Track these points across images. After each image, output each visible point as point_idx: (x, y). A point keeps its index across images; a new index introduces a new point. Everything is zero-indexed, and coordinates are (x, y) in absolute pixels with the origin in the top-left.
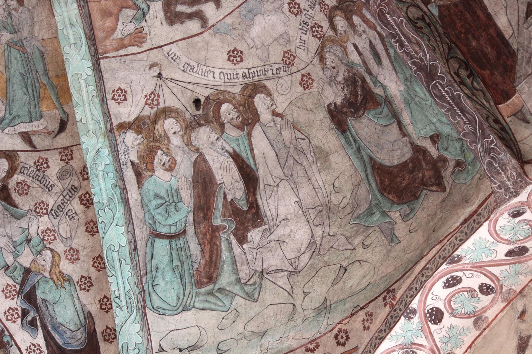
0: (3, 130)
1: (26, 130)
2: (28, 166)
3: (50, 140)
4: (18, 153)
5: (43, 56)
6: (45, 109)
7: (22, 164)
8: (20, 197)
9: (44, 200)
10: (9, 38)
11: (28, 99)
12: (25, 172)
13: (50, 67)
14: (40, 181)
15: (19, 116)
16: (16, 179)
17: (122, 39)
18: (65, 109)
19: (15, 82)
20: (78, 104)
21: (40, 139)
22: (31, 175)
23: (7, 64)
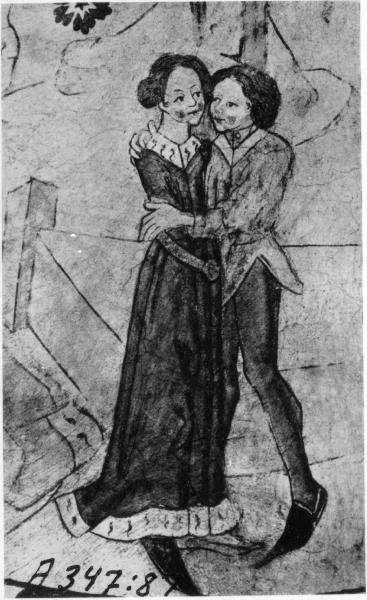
1: (167, 532)
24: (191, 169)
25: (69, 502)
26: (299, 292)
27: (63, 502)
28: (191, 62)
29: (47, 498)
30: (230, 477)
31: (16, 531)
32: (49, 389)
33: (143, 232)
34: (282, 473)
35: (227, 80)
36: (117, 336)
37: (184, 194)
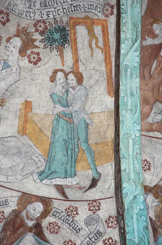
0: (41, 181)
1: (61, 184)
2: (60, 212)
3: (81, 194)
4: (53, 200)
5: (88, 127)
6: (79, 169)
7: (55, 209)
8: (51, 235)
9: (72, 240)
11: (67, 159)
12: (57, 216)
13: (91, 136)
14: (69, 224)
15: (56, 172)
16: (49, 220)
17: (152, 124)
20: (124, 157)
22: (62, 218)
23: (54, 131)
25: (36, 175)
26: (92, 125)
27: (34, 175)
28: (62, 70)
29: (30, 174)
30: (78, 171)
34: (90, 169)
37: (63, 103)
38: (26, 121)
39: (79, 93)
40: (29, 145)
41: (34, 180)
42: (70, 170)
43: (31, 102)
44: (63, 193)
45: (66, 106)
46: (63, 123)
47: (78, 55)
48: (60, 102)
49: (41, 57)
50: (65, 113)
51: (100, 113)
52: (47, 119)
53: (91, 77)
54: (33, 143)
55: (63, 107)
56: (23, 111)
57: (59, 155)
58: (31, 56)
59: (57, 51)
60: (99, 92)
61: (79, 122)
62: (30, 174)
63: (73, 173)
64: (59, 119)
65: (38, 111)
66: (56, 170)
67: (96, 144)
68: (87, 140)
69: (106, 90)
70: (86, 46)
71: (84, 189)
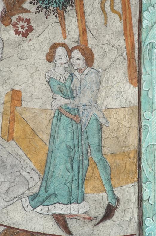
0: (34, 209)
1: (62, 212)
3: (91, 227)
5: (101, 128)
6: (89, 191)
10: (63, 104)
11: (71, 176)
13: (107, 143)
15: (55, 195)
18: (116, 193)
19: (58, 154)
21: (78, 225)
23: (53, 133)
24: (67, 83)
25: (26, 200)
26: (108, 126)
27: (23, 200)
28: (63, 45)
29: (18, 198)
30: (86, 193)
31: (6, 209)
32: (21, 162)
33: (52, 106)
34: (104, 192)
35: (76, 51)
36: (45, 143)
37: (66, 93)
38: (12, 120)
39: (88, 79)
40: (17, 155)
41: (24, 208)
42: (76, 191)
43: (19, 91)
44: (65, 227)
45: (70, 97)
46: (66, 121)
47: (86, 23)
48: (61, 91)
49: (33, 26)
50: (68, 108)
51: (118, 110)
52: (43, 115)
53: (104, 55)
54: (23, 151)
55: (66, 98)
56: (8, 105)
57: (61, 169)
58: (18, 25)
59: (56, 17)
60: (116, 79)
61: (88, 121)
62: (18, 198)
63: (80, 196)
64: (61, 116)
65: (30, 105)
66: (56, 192)
67: (114, 154)
68: (100, 148)
69: (127, 75)
70: (96, 10)
71: (95, 221)
